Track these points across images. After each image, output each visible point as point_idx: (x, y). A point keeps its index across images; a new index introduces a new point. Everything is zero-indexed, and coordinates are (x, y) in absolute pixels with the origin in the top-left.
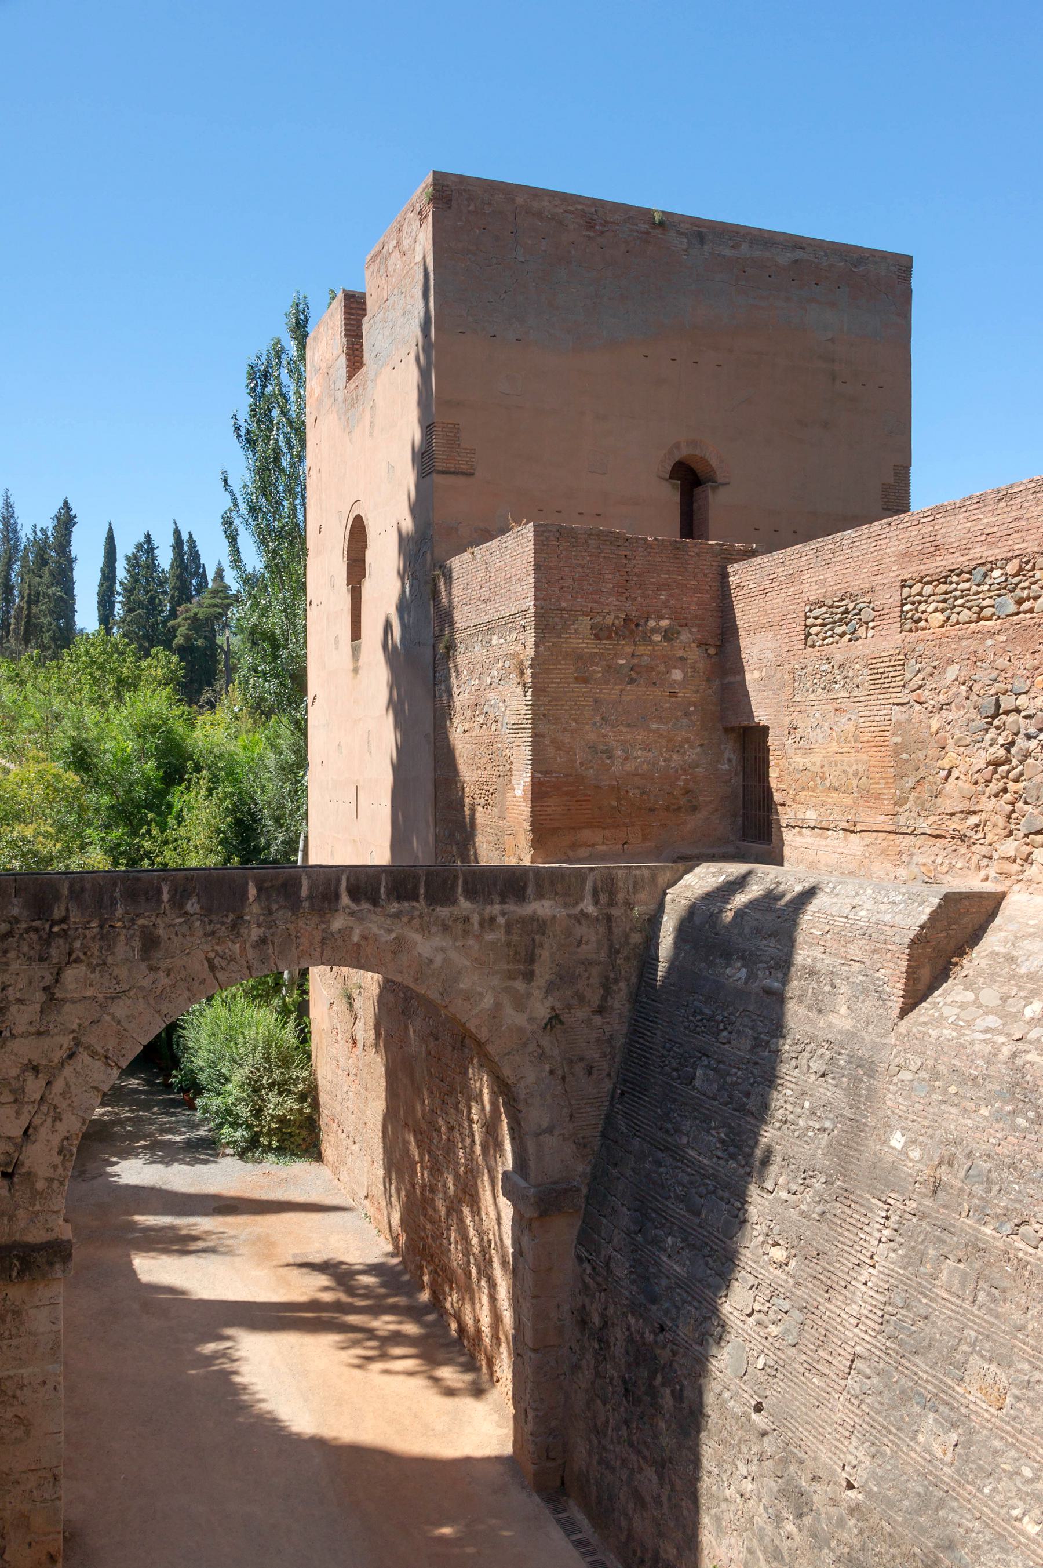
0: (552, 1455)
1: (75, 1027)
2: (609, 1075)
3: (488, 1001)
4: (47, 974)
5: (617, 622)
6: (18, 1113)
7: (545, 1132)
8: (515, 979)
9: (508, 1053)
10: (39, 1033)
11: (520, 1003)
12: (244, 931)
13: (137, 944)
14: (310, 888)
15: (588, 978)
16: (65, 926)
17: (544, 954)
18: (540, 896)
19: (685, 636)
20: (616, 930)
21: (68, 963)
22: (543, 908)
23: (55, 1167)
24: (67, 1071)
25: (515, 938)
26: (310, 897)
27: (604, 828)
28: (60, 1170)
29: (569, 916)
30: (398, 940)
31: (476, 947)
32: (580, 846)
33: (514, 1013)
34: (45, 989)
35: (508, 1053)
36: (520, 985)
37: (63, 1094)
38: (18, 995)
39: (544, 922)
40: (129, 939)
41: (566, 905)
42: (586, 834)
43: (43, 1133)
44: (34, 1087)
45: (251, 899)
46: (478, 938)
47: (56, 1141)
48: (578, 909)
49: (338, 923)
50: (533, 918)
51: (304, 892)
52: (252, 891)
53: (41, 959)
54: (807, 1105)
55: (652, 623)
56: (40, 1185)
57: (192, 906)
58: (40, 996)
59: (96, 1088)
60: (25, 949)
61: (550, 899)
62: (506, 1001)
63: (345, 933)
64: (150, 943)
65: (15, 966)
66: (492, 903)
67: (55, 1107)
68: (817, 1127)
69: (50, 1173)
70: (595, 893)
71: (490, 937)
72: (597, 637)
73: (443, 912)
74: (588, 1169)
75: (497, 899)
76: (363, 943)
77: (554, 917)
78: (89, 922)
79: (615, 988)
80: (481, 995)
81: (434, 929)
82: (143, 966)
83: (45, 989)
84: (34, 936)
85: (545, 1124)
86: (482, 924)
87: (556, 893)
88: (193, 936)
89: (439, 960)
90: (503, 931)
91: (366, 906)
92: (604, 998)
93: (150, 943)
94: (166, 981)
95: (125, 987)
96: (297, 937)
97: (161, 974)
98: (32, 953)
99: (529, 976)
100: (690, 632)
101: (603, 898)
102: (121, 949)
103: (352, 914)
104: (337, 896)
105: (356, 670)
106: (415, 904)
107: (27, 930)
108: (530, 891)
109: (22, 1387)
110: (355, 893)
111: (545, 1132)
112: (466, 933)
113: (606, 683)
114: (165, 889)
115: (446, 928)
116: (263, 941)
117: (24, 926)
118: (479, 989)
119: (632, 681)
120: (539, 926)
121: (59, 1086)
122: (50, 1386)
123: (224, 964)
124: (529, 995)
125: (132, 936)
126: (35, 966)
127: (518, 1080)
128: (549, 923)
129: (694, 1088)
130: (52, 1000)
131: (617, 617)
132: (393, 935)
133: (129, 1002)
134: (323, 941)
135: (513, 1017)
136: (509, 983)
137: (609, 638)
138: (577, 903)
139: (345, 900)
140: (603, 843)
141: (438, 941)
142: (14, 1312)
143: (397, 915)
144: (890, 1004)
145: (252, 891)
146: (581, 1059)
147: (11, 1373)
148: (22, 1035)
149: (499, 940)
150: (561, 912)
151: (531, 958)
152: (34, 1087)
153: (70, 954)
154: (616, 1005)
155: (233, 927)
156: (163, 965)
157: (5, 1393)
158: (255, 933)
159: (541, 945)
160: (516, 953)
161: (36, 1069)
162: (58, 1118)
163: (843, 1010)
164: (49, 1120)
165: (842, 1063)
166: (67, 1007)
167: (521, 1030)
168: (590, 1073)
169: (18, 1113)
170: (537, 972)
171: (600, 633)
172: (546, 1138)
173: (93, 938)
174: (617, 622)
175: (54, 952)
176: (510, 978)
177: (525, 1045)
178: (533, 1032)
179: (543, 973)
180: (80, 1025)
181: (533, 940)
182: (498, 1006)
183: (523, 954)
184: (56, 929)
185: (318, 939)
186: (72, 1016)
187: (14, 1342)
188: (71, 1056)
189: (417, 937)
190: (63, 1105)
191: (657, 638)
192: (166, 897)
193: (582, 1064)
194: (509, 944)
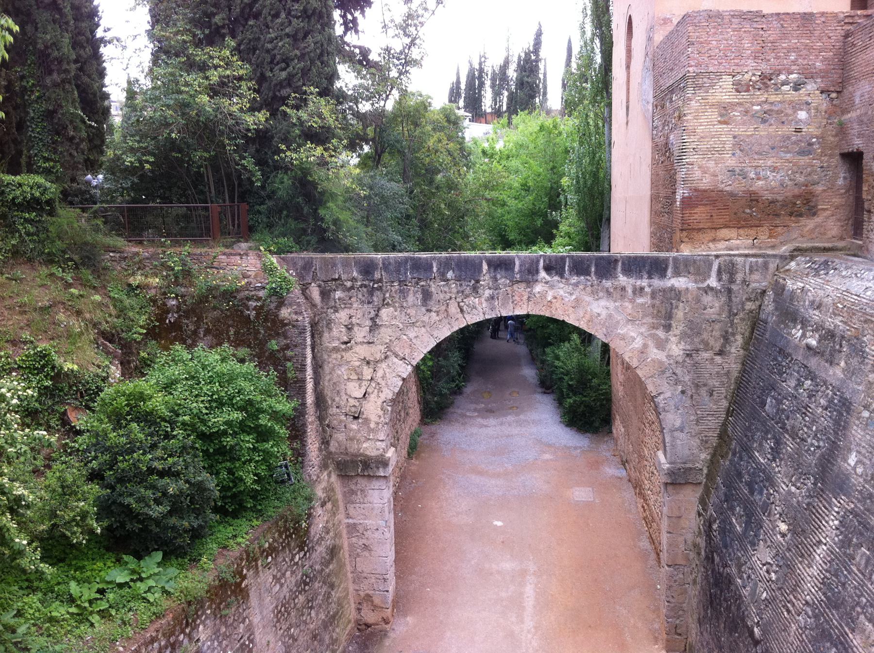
0: (679, 631)
1: (388, 341)
2: (726, 397)
3: (638, 343)
4: (372, 311)
5: (753, 78)
6: (360, 386)
7: (677, 430)
8: (657, 329)
9: (652, 377)
10: (369, 343)
11: (661, 345)
12: (480, 291)
13: (420, 296)
14: (521, 266)
15: (712, 331)
16: (380, 284)
17: (679, 314)
18: (677, 273)
19: (811, 87)
20: (734, 299)
21: (383, 305)
22: (680, 283)
23: (380, 417)
24: (384, 365)
25: (657, 302)
26: (520, 271)
27: (739, 228)
28: (382, 419)
29: (699, 288)
30: (577, 300)
31: (630, 307)
32: (719, 240)
33: (655, 351)
34: (371, 319)
35: (652, 377)
36: (661, 333)
37: (383, 377)
38: (358, 321)
39: (680, 292)
40: (415, 293)
41: (696, 282)
42: (724, 233)
43: (372, 397)
44: (367, 372)
45: (485, 271)
46: (632, 301)
47: (379, 403)
48: (705, 285)
49: (538, 288)
50: (672, 289)
51: (517, 269)
52: (485, 267)
53: (369, 303)
54: (814, 428)
55: (783, 77)
56: (372, 425)
57: (450, 275)
58: (368, 323)
59: (400, 376)
60: (360, 296)
61: (685, 276)
62: (650, 343)
63: (543, 295)
64: (427, 296)
65: (355, 305)
66: (641, 278)
67: (378, 384)
68: (816, 444)
69: (377, 420)
70: (719, 272)
71: (640, 300)
72: (737, 91)
73: (607, 284)
74: (709, 457)
75: (646, 276)
76: (554, 301)
77: (687, 289)
78: (393, 282)
79: (732, 339)
80: (634, 339)
81: (601, 294)
82: (423, 309)
83: (371, 319)
84: (365, 290)
85: (678, 424)
86: (634, 292)
87: (689, 273)
88: (450, 292)
89: (604, 313)
90: (649, 297)
91: (556, 278)
92: (723, 346)
93: (427, 296)
94: (438, 318)
95: (414, 320)
96: (513, 296)
97: (433, 314)
98: (363, 299)
99: (668, 328)
100: (815, 82)
101: (725, 277)
102: (411, 298)
103: (547, 283)
104: (537, 272)
105: (627, 123)
106: (588, 278)
107: (361, 286)
108: (669, 272)
109: (366, 530)
110: (548, 269)
111: (677, 430)
112: (623, 297)
113: (744, 123)
114: (435, 265)
115: (608, 293)
116: (492, 298)
117: (359, 283)
118: (632, 334)
119: (764, 121)
120: (676, 294)
121: (380, 373)
122: (380, 531)
123: (469, 310)
124: (667, 340)
125: (417, 292)
126: (366, 306)
127: (659, 394)
128: (683, 293)
129: (765, 411)
130: (374, 326)
131: (754, 75)
132: (574, 297)
133: (416, 329)
134: (529, 299)
135: (655, 354)
136: (654, 331)
137: (748, 90)
138: (705, 280)
139: (543, 274)
140: (737, 239)
141: (603, 303)
142: (362, 491)
143: (576, 285)
144: (867, 361)
145: (485, 267)
146: (705, 385)
147: (361, 522)
148: (362, 343)
149: (646, 303)
150: (692, 285)
151: (669, 316)
152: (367, 372)
153: (384, 300)
154: (733, 350)
155: (475, 289)
156: (434, 309)
157: (358, 531)
158: (487, 293)
159: (677, 307)
160: (659, 311)
161: (368, 363)
162: (380, 390)
163: (842, 364)
164: (376, 391)
165: (836, 401)
166: (383, 330)
167: (661, 362)
168: (711, 395)
169: (360, 386)
170: (674, 325)
171: (739, 87)
172: (676, 434)
173: (396, 292)
174: (753, 78)
175: (375, 299)
176: (654, 328)
177: (663, 372)
178: (670, 364)
179: (678, 328)
180: (390, 340)
181: (671, 304)
182: (645, 346)
183: (663, 313)
184: (376, 286)
185: (526, 297)
186: (385, 334)
187: (362, 506)
188: (386, 358)
189: (588, 299)
190: (383, 383)
191: (786, 88)
192: (435, 269)
193: (705, 388)
194: (653, 306)
